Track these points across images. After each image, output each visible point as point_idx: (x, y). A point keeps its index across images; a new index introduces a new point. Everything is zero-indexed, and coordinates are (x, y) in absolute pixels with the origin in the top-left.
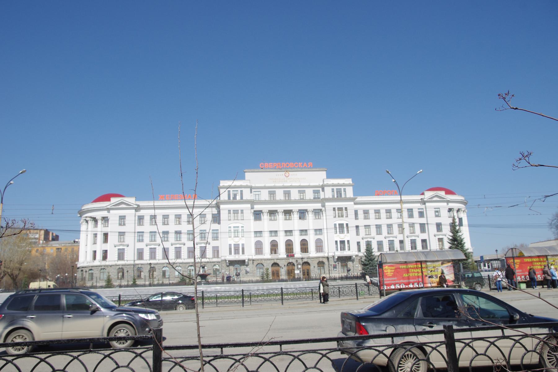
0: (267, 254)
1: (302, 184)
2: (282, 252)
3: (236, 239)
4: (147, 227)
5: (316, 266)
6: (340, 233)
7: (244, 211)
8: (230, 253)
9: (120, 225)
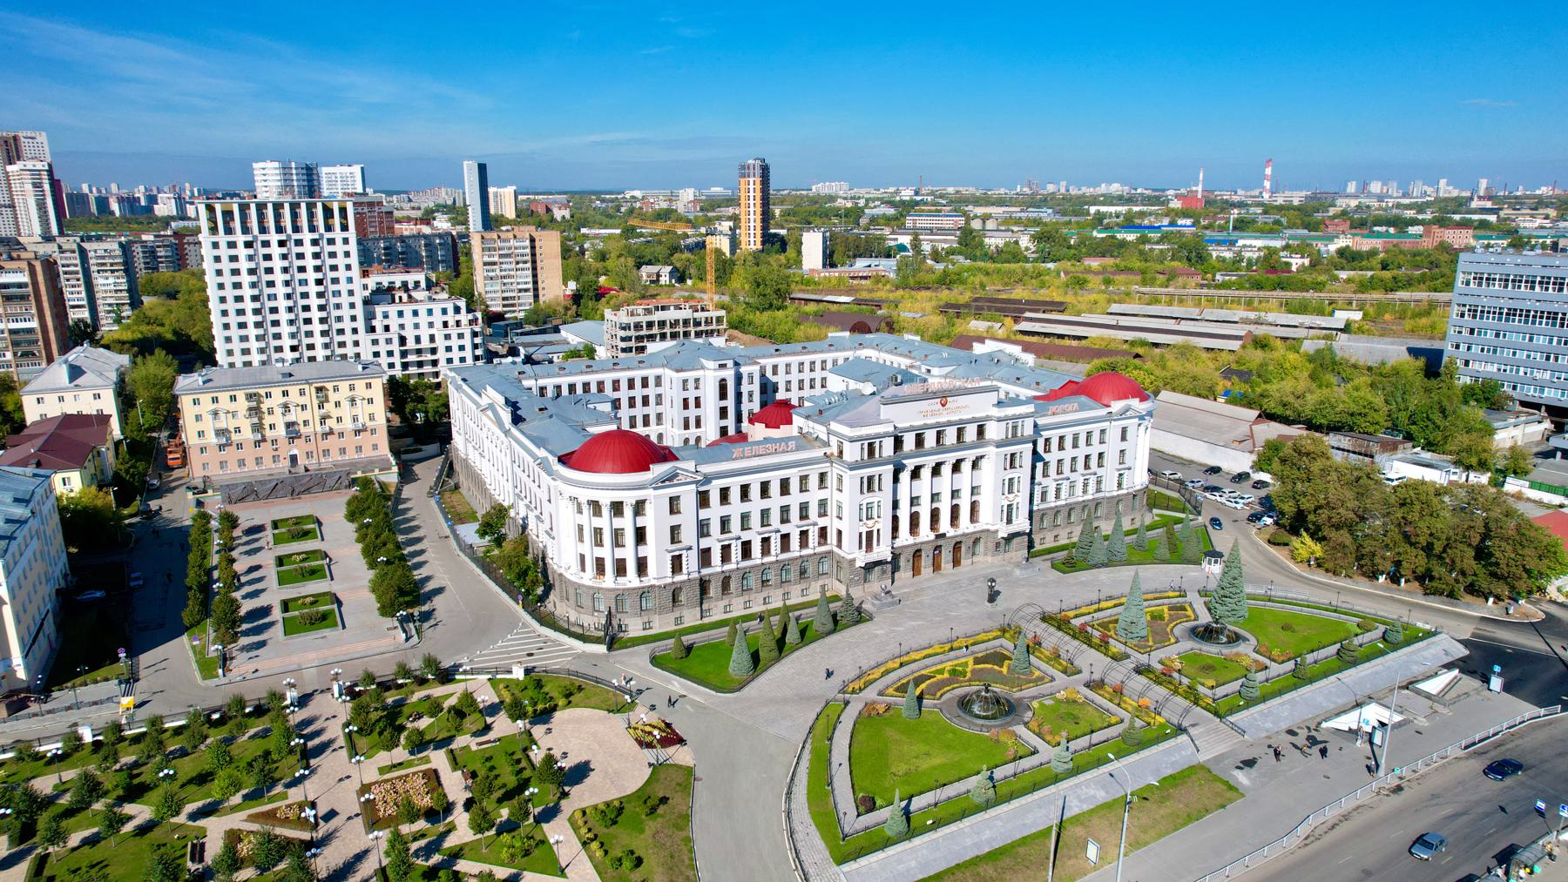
3: (870, 523)
4: (714, 512)
9: (672, 512)
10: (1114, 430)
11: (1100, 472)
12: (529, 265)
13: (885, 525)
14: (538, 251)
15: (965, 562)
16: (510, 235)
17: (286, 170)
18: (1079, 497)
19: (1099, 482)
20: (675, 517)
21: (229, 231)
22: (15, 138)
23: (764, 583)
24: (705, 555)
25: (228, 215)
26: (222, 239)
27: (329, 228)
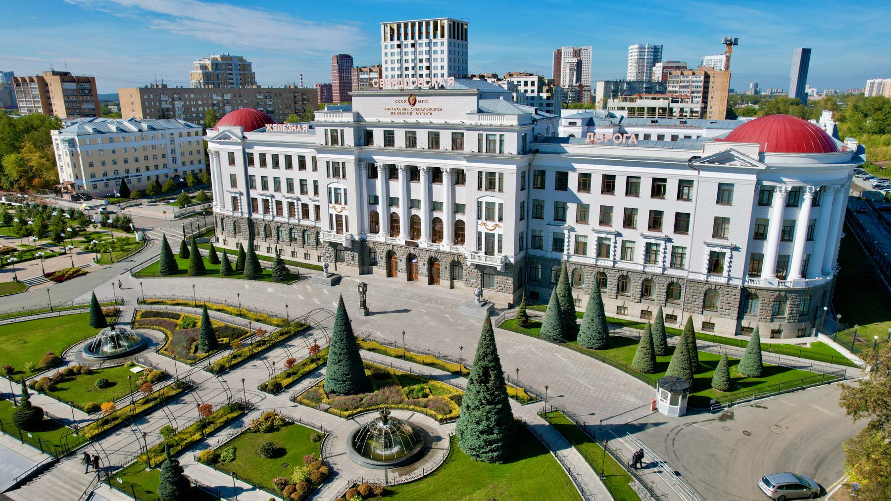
1: (435, 121)
4: (256, 171)
5: (448, 267)
10: (706, 183)
11: (679, 240)
12: (701, 95)
13: (350, 211)
14: (711, 84)
15: (445, 282)
16: (691, 73)
17: (641, 49)
18: (636, 263)
19: (677, 257)
20: (232, 167)
21: (392, 39)
22: (580, 50)
23: (292, 240)
24: (252, 204)
25: (392, 30)
26: (389, 43)
27: (435, 37)
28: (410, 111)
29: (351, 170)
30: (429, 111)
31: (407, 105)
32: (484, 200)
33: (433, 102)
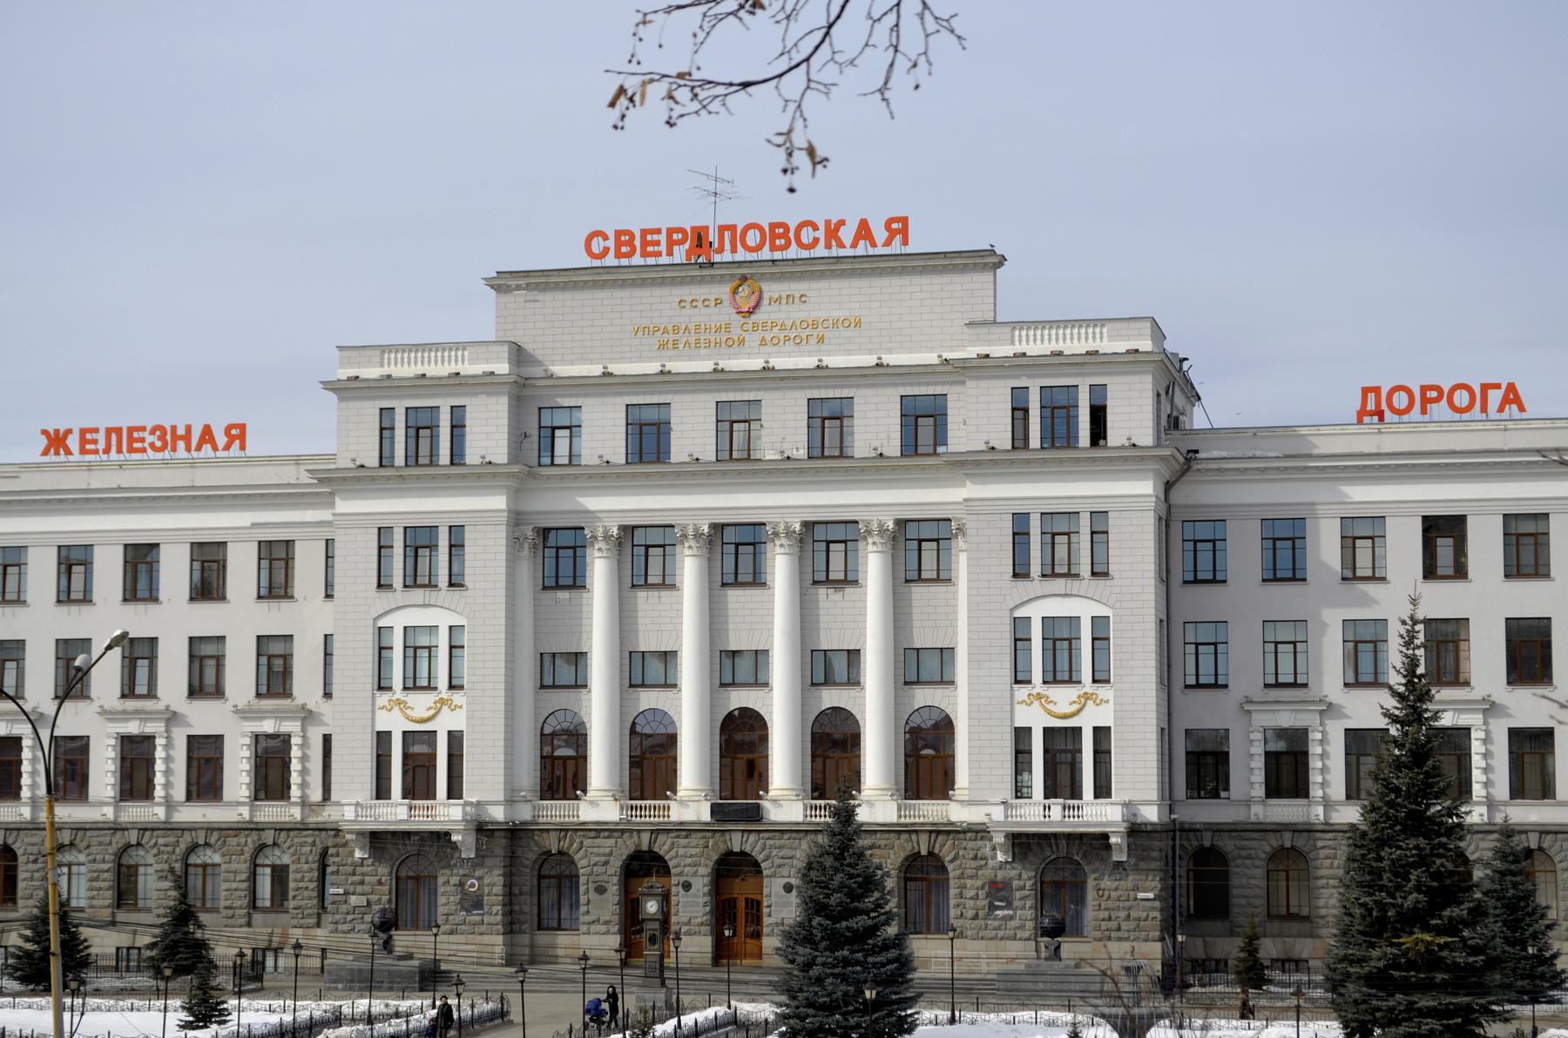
0: (601, 801)
1: (835, 361)
2: (692, 795)
3: (421, 703)
6: (1052, 679)
7: (470, 537)
8: (382, 792)
28: (736, 333)
29: (488, 556)
30: (814, 332)
31: (727, 313)
32: (1036, 613)
33: (829, 299)
